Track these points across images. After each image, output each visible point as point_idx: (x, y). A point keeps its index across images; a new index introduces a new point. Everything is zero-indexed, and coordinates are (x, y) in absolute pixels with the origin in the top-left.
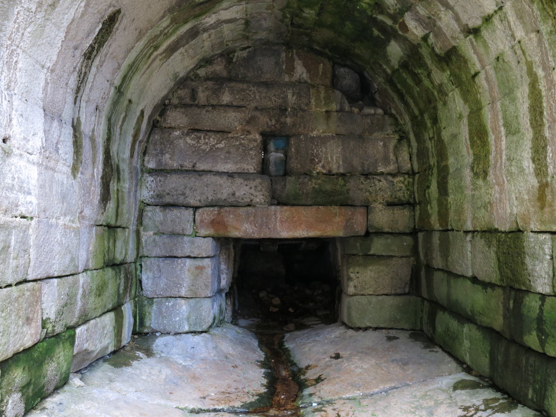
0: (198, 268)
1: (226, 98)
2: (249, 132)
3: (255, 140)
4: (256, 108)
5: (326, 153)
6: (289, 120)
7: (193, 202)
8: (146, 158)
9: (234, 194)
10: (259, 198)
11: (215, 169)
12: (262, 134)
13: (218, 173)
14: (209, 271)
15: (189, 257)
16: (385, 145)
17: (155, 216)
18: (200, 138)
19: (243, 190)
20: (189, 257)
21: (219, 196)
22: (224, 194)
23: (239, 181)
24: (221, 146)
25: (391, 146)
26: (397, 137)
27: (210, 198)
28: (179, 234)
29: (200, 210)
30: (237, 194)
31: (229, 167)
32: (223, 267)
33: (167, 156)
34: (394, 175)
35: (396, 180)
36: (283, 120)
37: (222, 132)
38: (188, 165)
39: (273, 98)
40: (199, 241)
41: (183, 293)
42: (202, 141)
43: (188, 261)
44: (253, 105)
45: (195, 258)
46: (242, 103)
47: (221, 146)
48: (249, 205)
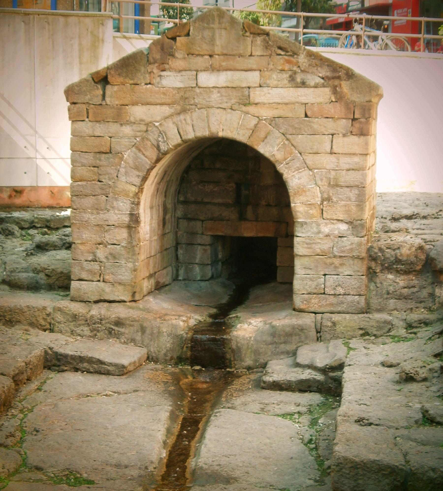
1: (218, 165)
7: (201, 218)
8: (180, 196)
9: (221, 215)
10: (234, 216)
13: (214, 204)
14: (209, 252)
15: (200, 244)
17: (184, 224)
18: (205, 185)
20: (200, 244)
24: (216, 189)
28: (195, 233)
29: (205, 222)
30: (223, 215)
31: (220, 200)
32: (220, 248)
33: (189, 195)
37: (217, 183)
38: (199, 199)
40: (205, 237)
41: (197, 261)
42: (206, 187)
43: (199, 247)
47: (216, 189)
48: (229, 220)
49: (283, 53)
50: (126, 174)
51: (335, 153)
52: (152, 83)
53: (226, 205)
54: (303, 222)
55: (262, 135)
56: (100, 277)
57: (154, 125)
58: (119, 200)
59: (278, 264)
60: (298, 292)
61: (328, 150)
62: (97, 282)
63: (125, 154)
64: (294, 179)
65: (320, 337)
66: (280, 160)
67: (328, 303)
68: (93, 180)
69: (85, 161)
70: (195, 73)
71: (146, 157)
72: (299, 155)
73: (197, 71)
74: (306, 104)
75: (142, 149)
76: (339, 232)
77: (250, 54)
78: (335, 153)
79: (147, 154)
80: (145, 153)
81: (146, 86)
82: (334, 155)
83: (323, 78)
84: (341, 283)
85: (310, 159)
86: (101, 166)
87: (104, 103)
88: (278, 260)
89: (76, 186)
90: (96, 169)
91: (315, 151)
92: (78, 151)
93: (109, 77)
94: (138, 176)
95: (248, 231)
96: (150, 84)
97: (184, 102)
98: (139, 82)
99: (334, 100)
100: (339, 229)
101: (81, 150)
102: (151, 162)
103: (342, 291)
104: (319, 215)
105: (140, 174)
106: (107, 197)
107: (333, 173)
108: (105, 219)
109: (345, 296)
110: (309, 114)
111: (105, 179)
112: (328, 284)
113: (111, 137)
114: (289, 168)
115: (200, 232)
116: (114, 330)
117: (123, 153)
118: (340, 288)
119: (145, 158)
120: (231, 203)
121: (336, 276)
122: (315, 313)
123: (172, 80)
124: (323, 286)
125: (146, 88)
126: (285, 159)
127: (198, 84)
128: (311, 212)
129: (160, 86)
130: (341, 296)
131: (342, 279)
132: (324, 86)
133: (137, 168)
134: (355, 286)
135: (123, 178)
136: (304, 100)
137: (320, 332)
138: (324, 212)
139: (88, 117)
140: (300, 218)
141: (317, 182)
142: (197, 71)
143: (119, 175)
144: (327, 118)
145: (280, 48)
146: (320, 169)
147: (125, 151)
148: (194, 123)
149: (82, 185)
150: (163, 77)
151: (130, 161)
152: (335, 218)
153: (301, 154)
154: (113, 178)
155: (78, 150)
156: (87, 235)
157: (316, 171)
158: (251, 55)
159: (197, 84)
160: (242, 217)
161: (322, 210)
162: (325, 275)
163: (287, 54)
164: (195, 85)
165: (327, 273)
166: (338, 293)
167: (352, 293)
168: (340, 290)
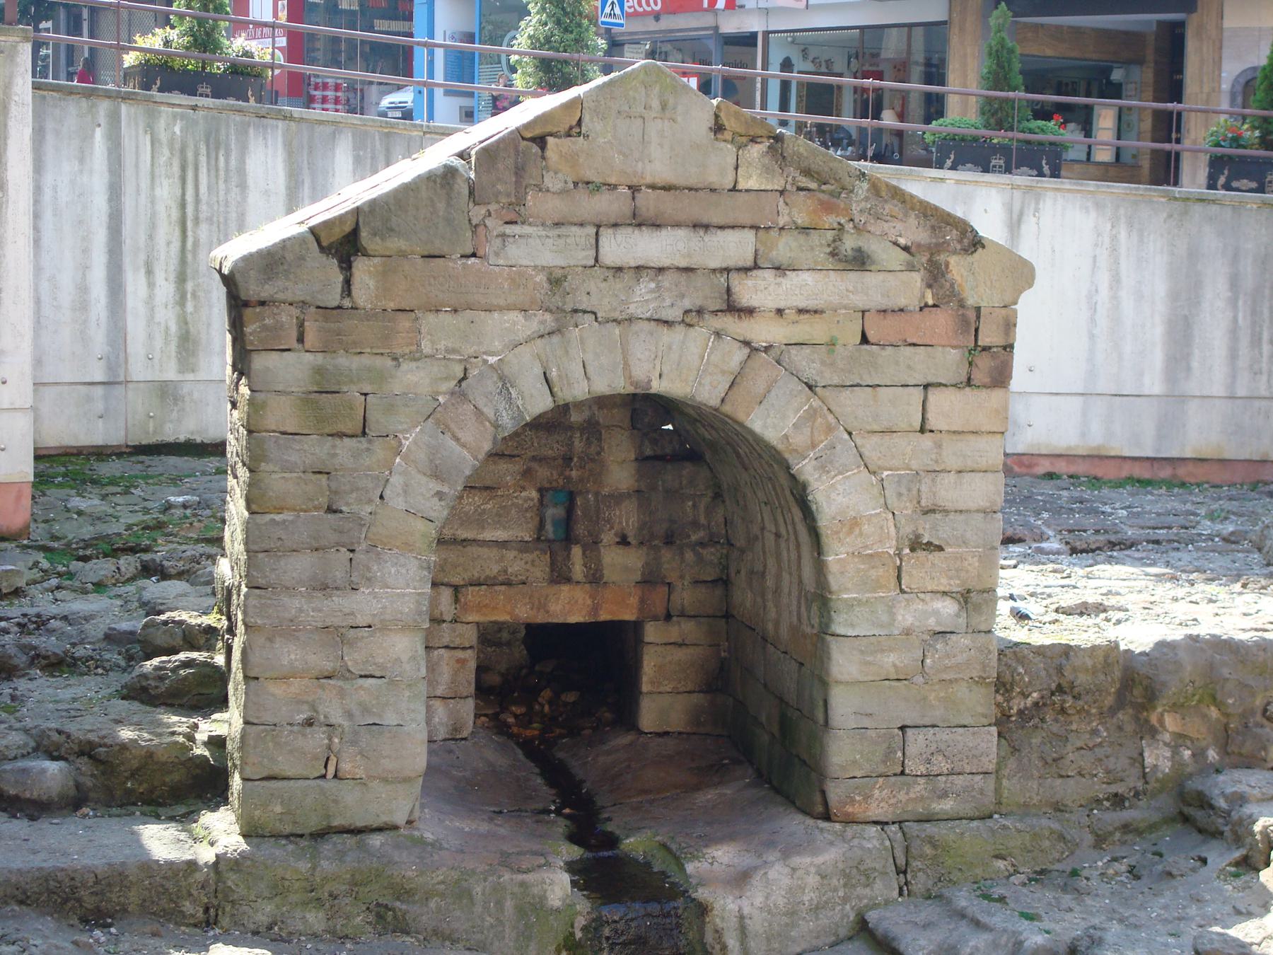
0: (458, 661)
2: (523, 488)
3: (532, 500)
4: (534, 458)
5: (620, 517)
6: (574, 474)
7: (456, 580)
9: (506, 572)
11: (480, 537)
12: (541, 491)
16: (694, 506)
19: (516, 565)
21: (488, 572)
22: (493, 569)
23: (511, 554)
25: (702, 507)
26: (710, 493)
27: (476, 575)
30: (510, 570)
31: (501, 535)
34: (702, 544)
35: (704, 552)
36: (567, 473)
39: (555, 446)
44: (530, 454)
45: (455, 648)
46: (516, 452)
49: (813, 185)
50: (405, 492)
51: (932, 431)
52: (480, 253)
53: (523, 547)
54: (854, 599)
55: (760, 386)
56: (326, 767)
57: (485, 361)
58: (386, 557)
59: (645, 688)
60: (839, 774)
61: (917, 426)
62: (318, 781)
63: (407, 439)
64: (838, 495)
65: (906, 884)
66: (800, 450)
67: (912, 795)
68: (317, 508)
69: (294, 457)
70: (593, 230)
71: (463, 446)
72: (846, 436)
73: (599, 226)
74: (863, 312)
75: (452, 426)
76: (938, 623)
77: (731, 186)
78: (932, 431)
79: (466, 436)
80: (460, 435)
81: (464, 260)
82: (928, 434)
83: (906, 249)
84: (943, 747)
85: (870, 446)
86: (336, 470)
87: (347, 303)
88: (645, 679)
89: (266, 524)
90: (324, 478)
91: (884, 425)
92: (274, 431)
93: (364, 234)
94: (440, 495)
95: (569, 606)
96: (474, 255)
97: (559, 303)
98: (445, 250)
99: (931, 302)
100: (936, 613)
101: (282, 429)
102: (475, 458)
103: (945, 767)
104: (893, 581)
105: (446, 489)
106: (352, 551)
107: (927, 480)
108: (347, 610)
109: (950, 778)
110: (871, 335)
111: (347, 504)
112: (911, 750)
113: (366, 395)
114: (823, 469)
115: (448, 617)
116: (393, 910)
117: (401, 436)
118: (940, 758)
119: (458, 448)
120: (527, 538)
121: (932, 731)
122: (883, 824)
123: (533, 251)
124: (900, 754)
125: (465, 266)
126: (814, 446)
127: (600, 258)
128: (873, 573)
129: (501, 262)
130: (944, 778)
131: (945, 737)
132: (911, 268)
133: (436, 474)
134: (974, 752)
135: (397, 501)
136: (860, 301)
137: (905, 872)
138: (903, 575)
139: (301, 340)
140: (847, 590)
141: (889, 502)
142: (599, 226)
143: (387, 493)
144: (914, 345)
145: (807, 172)
146: (898, 469)
147: (406, 431)
148: (589, 358)
149: (284, 521)
150: (511, 240)
151: (422, 456)
152: (929, 589)
153: (850, 434)
154: (370, 501)
155: (274, 428)
156: (293, 657)
157: (886, 473)
158: (734, 189)
159: (596, 260)
160: (560, 576)
161: (899, 569)
162: (902, 728)
163: (824, 187)
164: (592, 262)
165: (908, 723)
166: (935, 770)
167: (968, 769)
168: (941, 765)
